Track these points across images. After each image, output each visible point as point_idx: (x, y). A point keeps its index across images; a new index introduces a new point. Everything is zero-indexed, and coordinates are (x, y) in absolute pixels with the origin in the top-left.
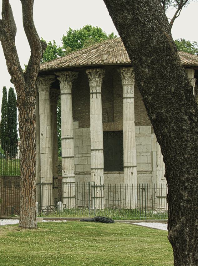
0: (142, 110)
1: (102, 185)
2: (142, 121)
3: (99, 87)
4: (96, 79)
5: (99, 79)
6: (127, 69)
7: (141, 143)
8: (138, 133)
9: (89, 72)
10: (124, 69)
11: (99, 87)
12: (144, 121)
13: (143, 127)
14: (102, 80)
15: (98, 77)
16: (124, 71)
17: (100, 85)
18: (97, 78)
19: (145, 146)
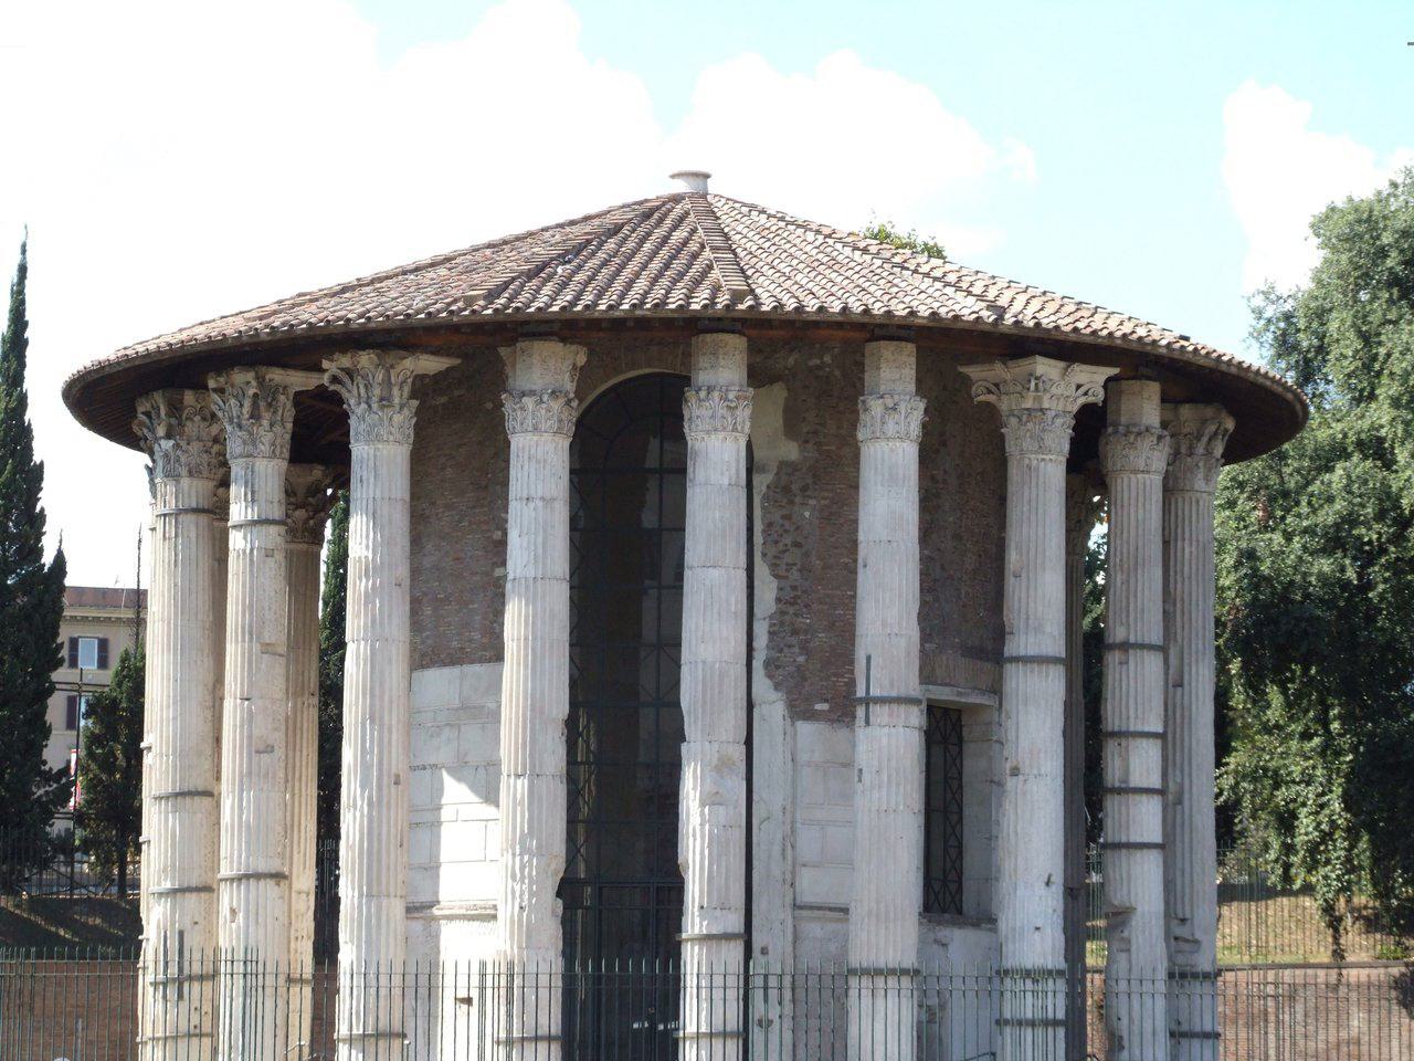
0: (478, 578)
1: (173, 971)
2: (476, 636)
3: (178, 482)
4: (163, 442)
5: (172, 442)
6: (222, 380)
7: (466, 754)
8: (457, 703)
9: (148, 414)
10: (212, 384)
11: (178, 482)
12: (484, 640)
13: (476, 668)
14: (195, 447)
15: (161, 431)
16: (220, 391)
17: (184, 472)
18: (168, 436)
19: (481, 771)
